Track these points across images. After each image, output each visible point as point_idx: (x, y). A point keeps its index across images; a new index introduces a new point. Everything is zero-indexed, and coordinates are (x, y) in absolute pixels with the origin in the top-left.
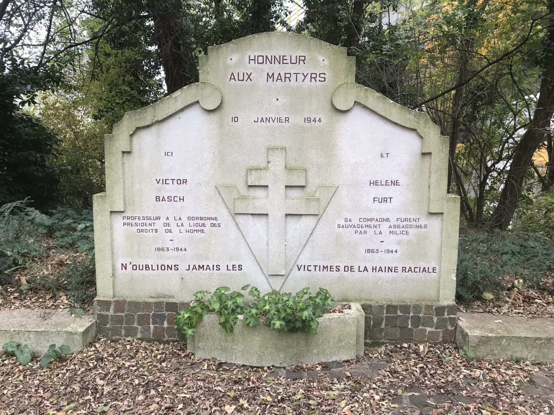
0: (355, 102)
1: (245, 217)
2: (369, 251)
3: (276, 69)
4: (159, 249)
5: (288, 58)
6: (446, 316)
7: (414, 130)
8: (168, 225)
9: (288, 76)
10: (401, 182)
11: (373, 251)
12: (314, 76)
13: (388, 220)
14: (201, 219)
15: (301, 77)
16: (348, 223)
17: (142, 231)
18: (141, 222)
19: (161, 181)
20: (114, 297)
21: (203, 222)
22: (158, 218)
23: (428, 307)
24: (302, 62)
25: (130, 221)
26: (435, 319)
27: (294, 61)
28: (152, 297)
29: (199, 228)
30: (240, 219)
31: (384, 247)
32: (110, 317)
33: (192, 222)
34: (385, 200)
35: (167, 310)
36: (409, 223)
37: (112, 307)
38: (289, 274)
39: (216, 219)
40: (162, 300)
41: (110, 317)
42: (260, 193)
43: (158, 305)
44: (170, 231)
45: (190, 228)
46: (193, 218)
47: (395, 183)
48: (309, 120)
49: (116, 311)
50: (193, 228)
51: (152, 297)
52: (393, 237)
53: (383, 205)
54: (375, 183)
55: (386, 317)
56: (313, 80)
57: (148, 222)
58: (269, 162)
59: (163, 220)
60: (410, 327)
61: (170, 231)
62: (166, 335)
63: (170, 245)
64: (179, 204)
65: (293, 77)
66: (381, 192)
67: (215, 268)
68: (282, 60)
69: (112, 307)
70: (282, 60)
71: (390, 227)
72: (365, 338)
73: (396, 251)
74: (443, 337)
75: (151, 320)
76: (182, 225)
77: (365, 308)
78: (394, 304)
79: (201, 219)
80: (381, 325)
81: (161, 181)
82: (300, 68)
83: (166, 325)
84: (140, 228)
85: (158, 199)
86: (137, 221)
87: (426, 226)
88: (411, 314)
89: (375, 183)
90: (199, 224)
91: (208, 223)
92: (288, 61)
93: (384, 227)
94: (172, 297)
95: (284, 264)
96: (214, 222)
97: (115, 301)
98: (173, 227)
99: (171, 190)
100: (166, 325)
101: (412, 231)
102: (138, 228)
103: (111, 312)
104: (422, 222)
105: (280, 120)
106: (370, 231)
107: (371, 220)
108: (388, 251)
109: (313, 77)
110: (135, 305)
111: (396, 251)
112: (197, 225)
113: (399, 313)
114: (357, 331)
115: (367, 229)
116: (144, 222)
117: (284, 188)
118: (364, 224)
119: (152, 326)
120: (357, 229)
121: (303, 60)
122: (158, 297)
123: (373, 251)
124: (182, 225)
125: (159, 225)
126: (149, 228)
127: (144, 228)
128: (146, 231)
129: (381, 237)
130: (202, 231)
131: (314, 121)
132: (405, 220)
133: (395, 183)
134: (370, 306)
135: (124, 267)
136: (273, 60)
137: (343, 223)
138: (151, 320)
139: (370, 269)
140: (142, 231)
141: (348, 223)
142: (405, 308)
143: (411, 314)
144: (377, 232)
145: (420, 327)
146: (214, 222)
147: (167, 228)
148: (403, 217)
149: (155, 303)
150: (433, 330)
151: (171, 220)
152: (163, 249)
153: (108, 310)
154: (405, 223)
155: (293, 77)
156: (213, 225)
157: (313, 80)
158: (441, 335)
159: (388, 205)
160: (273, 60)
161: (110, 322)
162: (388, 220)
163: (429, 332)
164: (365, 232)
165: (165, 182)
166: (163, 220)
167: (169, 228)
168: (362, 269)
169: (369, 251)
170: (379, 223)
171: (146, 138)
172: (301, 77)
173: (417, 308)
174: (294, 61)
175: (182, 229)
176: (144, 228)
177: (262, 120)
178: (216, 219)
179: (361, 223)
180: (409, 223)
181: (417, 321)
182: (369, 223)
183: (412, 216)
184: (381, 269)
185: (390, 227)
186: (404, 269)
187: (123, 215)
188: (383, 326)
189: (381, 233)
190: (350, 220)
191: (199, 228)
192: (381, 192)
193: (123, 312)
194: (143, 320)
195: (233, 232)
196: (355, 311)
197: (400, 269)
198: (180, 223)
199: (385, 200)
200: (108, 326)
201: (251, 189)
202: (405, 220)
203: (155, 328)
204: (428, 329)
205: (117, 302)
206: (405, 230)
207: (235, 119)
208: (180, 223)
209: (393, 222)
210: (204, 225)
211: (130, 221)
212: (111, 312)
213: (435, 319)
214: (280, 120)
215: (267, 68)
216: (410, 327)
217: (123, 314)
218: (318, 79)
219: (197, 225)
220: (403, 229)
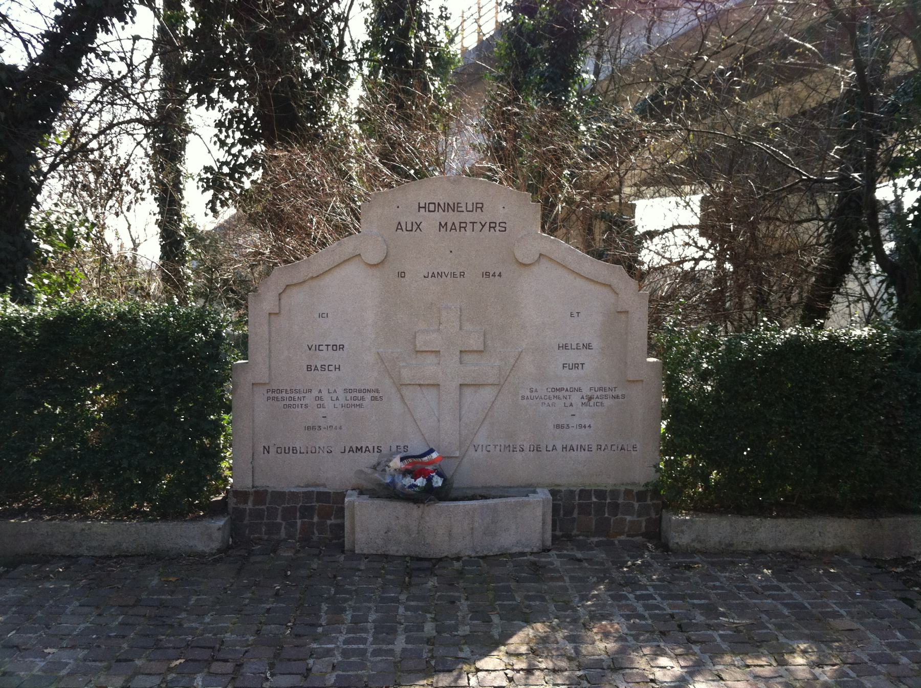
0: (541, 255)
1: (411, 388)
2: (558, 426)
3: (451, 217)
4: (308, 428)
5: (463, 205)
6: (649, 502)
7: (610, 286)
8: (320, 398)
9: (463, 225)
10: (595, 344)
11: (562, 427)
12: (492, 225)
13: (579, 390)
14: (360, 391)
15: (478, 227)
16: (534, 394)
17: (289, 406)
18: (288, 396)
19: (313, 348)
20: (253, 487)
21: (362, 394)
22: (310, 391)
23: (628, 493)
24: (479, 210)
25: (275, 395)
26: (636, 505)
27: (470, 208)
28: (299, 486)
29: (357, 402)
30: (406, 392)
31: (575, 421)
32: (248, 511)
33: (349, 395)
34: (576, 366)
35: (317, 501)
36: (604, 393)
37: (251, 498)
38: (464, 456)
39: (377, 391)
40: (310, 489)
41: (248, 511)
42: (431, 359)
43: (308, 495)
44: (323, 406)
45: (347, 402)
46: (350, 391)
47: (588, 346)
48: (487, 274)
49: (255, 503)
50: (349, 402)
51: (299, 486)
52: (586, 409)
53: (574, 373)
54: (565, 347)
55: (580, 505)
56: (492, 230)
57: (297, 396)
58: (440, 324)
59: (315, 393)
60: (606, 515)
61: (323, 406)
62: (316, 532)
63: (322, 422)
64: (333, 375)
65: (470, 226)
66: (572, 357)
67: (376, 450)
68: (454, 207)
69: (251, 498)
70: (454, 207)
71: (583, 398)
72: (554, 530)
73: (590, 426)
74: (646, 526)
75: (298, 514)
76: (337, 399)
77: (554, 493)
78: (587, 488)
79: (360, 391)
80: (571, 513)
81: (313, 348)
82: (476, 216)
83: (316, 519)
84: (288, 403)
85: (309, 368)
86: (284, 394)
87: (623, 396)
88: (608, 501)
89: (565, 347)
90: (356, 396)
91: (368, 396)
92: (464, 209)
93: (575, 398)
94: (324, 486)
95: (458, 444)
96: (376, 394)
97: (255, 492)
98: (327, 402)
99: (326, 357)
100: (316, 519)
101: (608, 402)
102: (284, 403)
103: (250, 505)
104: (619, 392)
105: (454, 275)
106: (560, 403)
107: (561, 389)
108: (580, 426)
109: (492, 226)
110: (279, 496)
111: (590, 426)
112: (355, 398)
113: (594, 499)
114: (544, 515)
115: (555, 400)
116: (292, 395)
117: (458, 353)
118: (552, 394)
119: (299, 522)
120: (544, 401)
121: (481, 208)
122: (307, 486)
123: (562, 427)
124: (337, 399)
125: (309, 399)
126: (297, 403)
127: (292, 403)
128: (294, 406)
129: (572, 410)
130: (360, 406)
131: (494, 275)
132: (600, 389)
133: (588, 346)
134: (560, 491)
135: (267, 450)
136: (448, 207)
137: (528, 393)
138: (298, 514)
139: (559, 447)
140: (289, 406)
141: (534, 394)
142: (601, 494)
143: (608, 501)
144: (568, 404)
145: (619, 516)
146: (376, 394)
147: (319, 402)
148: (597, 386)
149: (304, 493)
150: (635, 518)
151: (325, 392)
152: (314, 428)
153: (246, 502)
154: (599, 393)
155: (470, 226)
156: (374, 399)
157: (492, 230)
158: (644, 524)
159: (580, 372)
160: (448, 207)
161: (247, 518)
162: (579, 390)
163: (630, 521)
164: (554, 405)
165: (318, 348)
166: (315, 393)
167: (322, 403)
168: (550, 448)
169: (558, 426)
170: (569, 393)
171: (297, 297)
172: (478, 227)
173: (615, 493)
174: (470, 208)
175: (337, 403)
176: (292, 403)
177: (433, 276)
178: (377, 391)
179: (549, 394)
180: (604, 393)
181: (615, 507)
182: (557, 393)
183: (607, 386)
184: (572, 449)
185: (583, 398)
186: (599, 447)
187: (268, 387)
188: (575, 515)
189: (571, 405)
190: (536, 391)
191: (357, 402)
192: (572, 357)
193: (265, 504)
194: (289, 514)
195: (397, 406)
196: (543, 495)
197: (594, 448)
198: (334, 396)
199: (576, 366)
200: (245, 522)
201: (419, 355)
202: (600, 389)
203: (303, 524)
204: (628, 518)
205: (257, 493)
206: (600, 400)
207: (402, 275)
208: (334, 396)
209: (586, 392)
210: (363, 399)
211: (275, 395)
212: (250, 505)
213: (636, 505)
214: (454, 275)
215: (439, 216)
216: (606, 515)
217: (264, 507)
218: (498, 228)
219: (355, 398)
220: (598, 400)
